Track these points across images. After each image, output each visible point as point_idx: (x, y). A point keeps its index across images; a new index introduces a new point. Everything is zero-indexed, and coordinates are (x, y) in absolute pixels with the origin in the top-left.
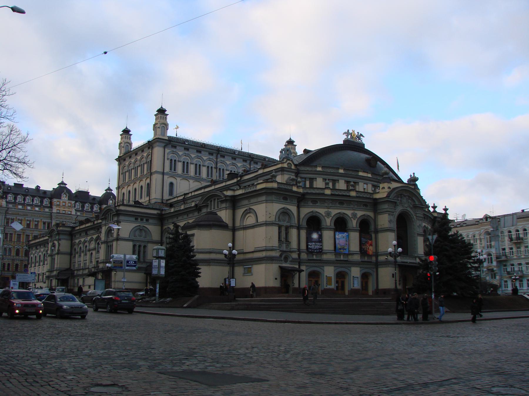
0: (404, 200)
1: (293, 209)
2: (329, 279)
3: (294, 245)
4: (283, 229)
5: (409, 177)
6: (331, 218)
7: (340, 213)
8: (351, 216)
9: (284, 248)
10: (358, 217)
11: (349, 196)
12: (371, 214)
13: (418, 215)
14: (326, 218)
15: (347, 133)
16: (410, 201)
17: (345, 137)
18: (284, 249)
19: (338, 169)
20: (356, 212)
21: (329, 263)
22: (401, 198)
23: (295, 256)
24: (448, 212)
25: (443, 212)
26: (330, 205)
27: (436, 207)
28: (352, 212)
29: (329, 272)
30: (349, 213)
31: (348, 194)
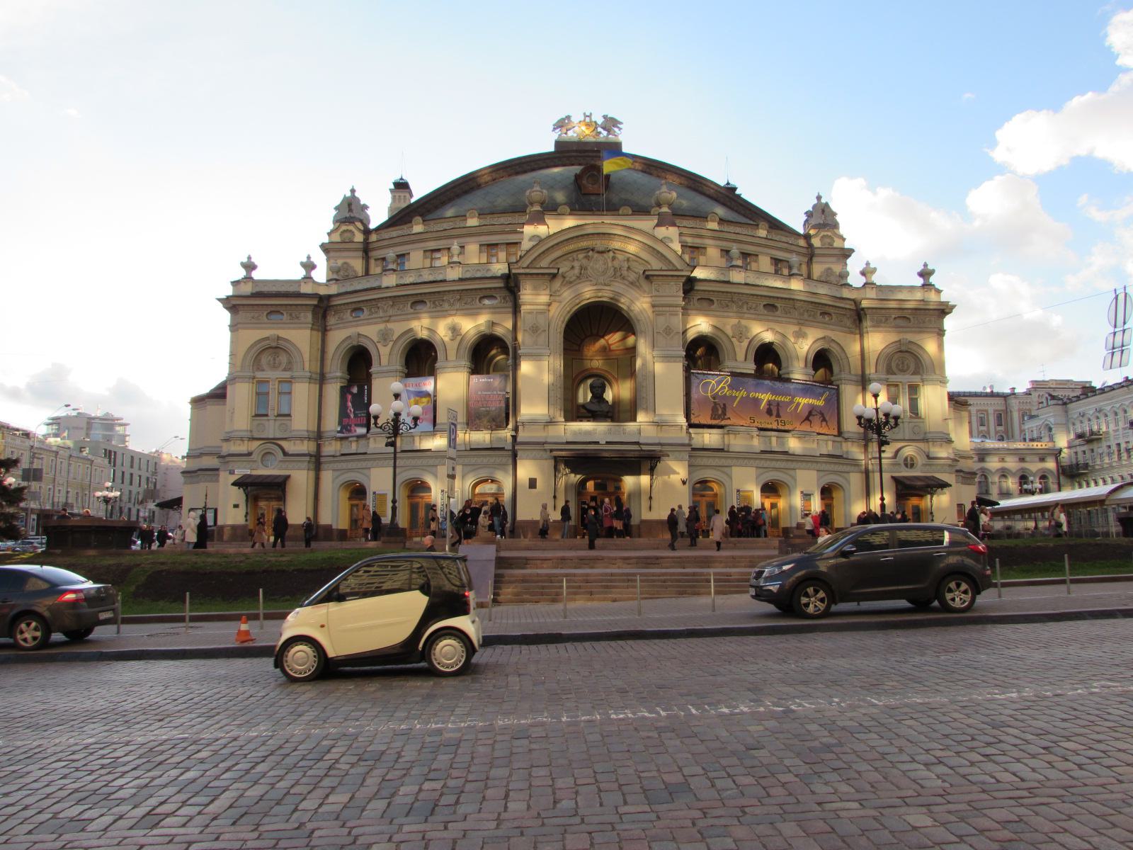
1: (301, 337)
2: (380, 498)
3: (302, 420)
4: (273, 389)
5: (816, 202)
6: (391, 343)
9: (271, 428)
11: (444, 281)
14: (379, 346)
15: (562, 124)
17: (555, 136)
18: (271, 436)
19: (463, 217)
22: (587, 257)
23: (306, 447)
24: (932, 280)
26: (391, 312)
27: (874, 271)
31: (440, 278)
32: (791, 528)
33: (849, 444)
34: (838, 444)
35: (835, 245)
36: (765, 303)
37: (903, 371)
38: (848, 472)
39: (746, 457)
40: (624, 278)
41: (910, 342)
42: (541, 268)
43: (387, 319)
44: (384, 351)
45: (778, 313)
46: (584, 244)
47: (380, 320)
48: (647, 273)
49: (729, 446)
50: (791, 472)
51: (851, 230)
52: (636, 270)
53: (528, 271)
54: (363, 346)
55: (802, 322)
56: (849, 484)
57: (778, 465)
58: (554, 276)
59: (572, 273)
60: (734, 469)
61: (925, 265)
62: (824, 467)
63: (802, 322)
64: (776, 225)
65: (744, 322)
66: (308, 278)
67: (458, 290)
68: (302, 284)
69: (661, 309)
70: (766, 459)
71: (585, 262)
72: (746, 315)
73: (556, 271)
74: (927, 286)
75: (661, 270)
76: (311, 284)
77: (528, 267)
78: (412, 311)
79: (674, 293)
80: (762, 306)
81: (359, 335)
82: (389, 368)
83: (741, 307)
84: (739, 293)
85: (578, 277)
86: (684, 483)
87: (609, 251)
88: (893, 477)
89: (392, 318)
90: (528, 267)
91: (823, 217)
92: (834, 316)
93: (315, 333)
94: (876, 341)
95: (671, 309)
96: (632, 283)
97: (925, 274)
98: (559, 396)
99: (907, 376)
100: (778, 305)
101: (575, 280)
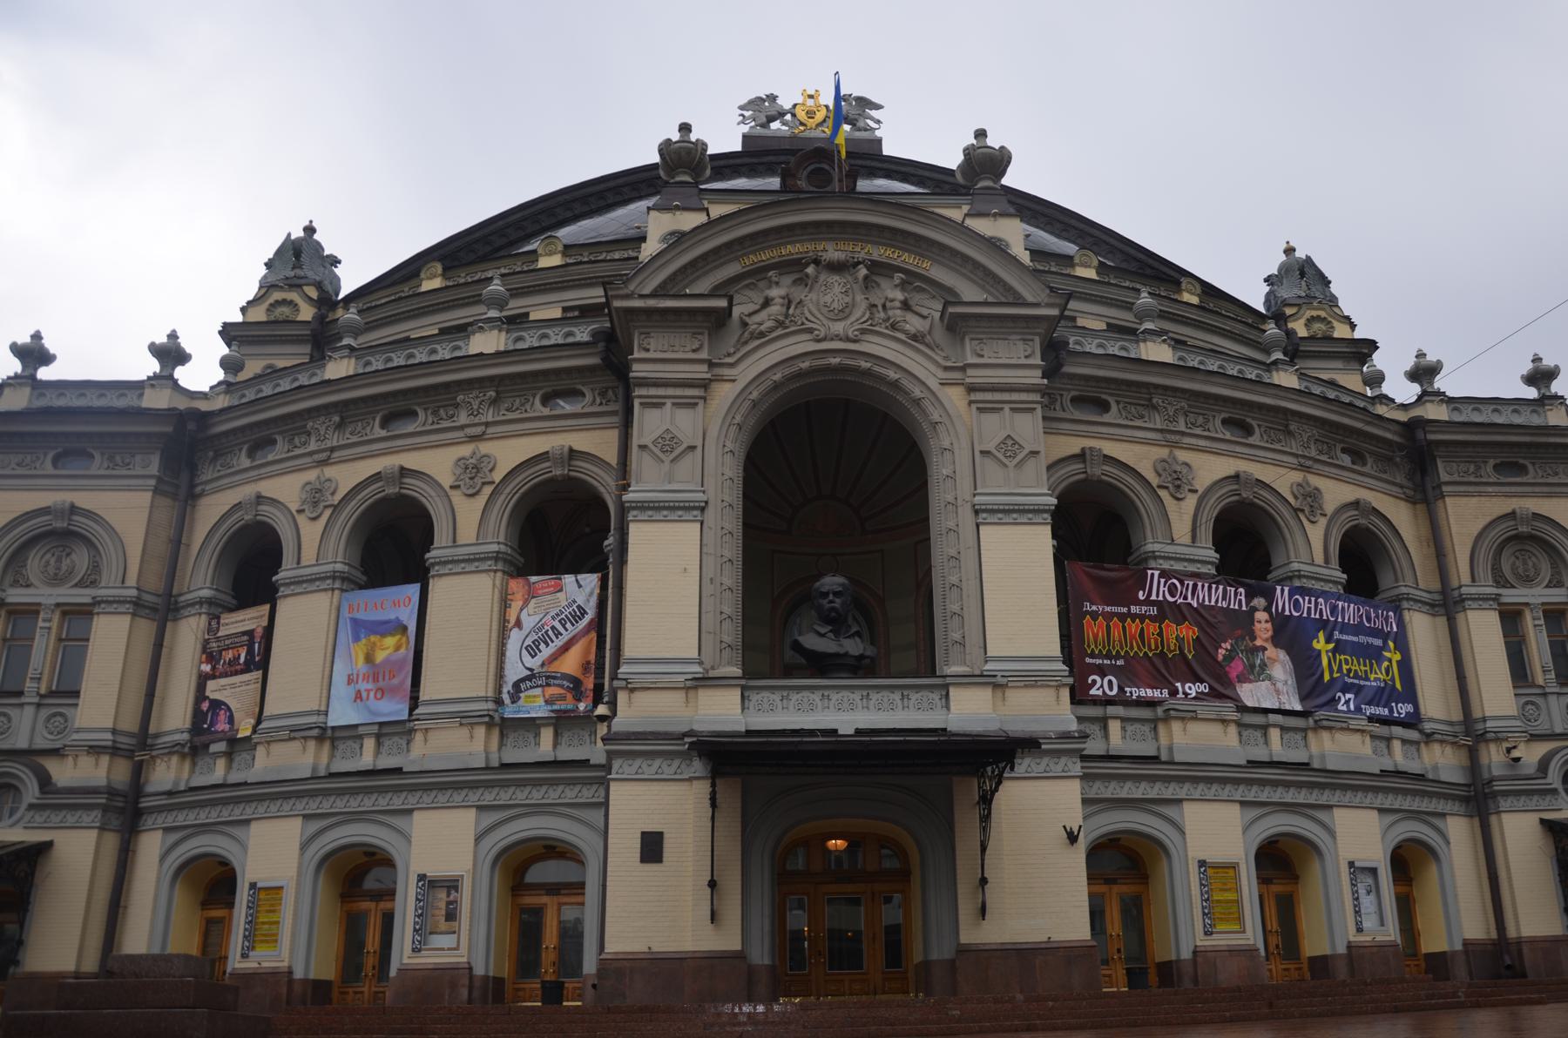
0: (833, 291)
6: (328, 512)
7: (377, 477)
8: (446, 482)
10: (498, 476)
12: (600, 442)
13: (975, 376)
14: (301, 519)
16: (899, 295)
20: (485, 448)
21: (279, 793)
22: (802, 281)
24: (1557, 387)
25: (1531, 393)
28: (465, 450)
29: (273, 853)
30: (437, 463)
32: (1334, 957)
33: (1436, 747)
34: (1413, 749)
35: (1336, 335)
36: (1224, 415)
37: (1527, 580)
38: (1443, 815)
39: (1207, 777)
40: (893, 327)
41: (1536, 516)
42: (686, 296)
43: (323, 456)
44: (311, 532)
45: (1255, 439)
46: (793, 250)
47: (308, 460)
48: (951, 310)
49: (1170, 749)
50: (1321, 815)
51: (1363, 305)
52: (925, 312)
53: (651, 303)
54: (264, 523)
55: (1309, 463)
56: (1448, 843)
57: (1290, 796)
58: (717, 321)
59: (763, 315)
60: (1189, 809)
61: (1536, 359)
62: (1389, 801)
63: (1309, 463)
64: (1209, 290)
65: (1182, 456)
66: (165, 379)
67: (491, 379)
68: (148, 391)
69: (988, 396)
70: (1263, 783)
71: (799, 293)
72: (1187, 440)
73: (723, 303)
74: (1547, 400)
75: (985, 304)
76: (167, 392)
77: (654, 295)
78: (383, 433)
79: (1017, 361)
80: (1218, 422)
81: (260, 499)
82: (316, 570)
83: (1173, 420)
84: (1166, 388)
85: (780, 324)
86: (1072, 838)
87: (859, 263)
88: (1542, 821)
89: (336, 454)
90: (654, 295)
91: (1302, 278)
92: (1370, 461)
93: (165, 502)
94: (1468, 515)
95: (1015, 396)
96: (914, 337)
97: (1541, 376)
98: (727, 610)
99: (1539, 590)
100: (1254, 423)
101: (772, 330)
